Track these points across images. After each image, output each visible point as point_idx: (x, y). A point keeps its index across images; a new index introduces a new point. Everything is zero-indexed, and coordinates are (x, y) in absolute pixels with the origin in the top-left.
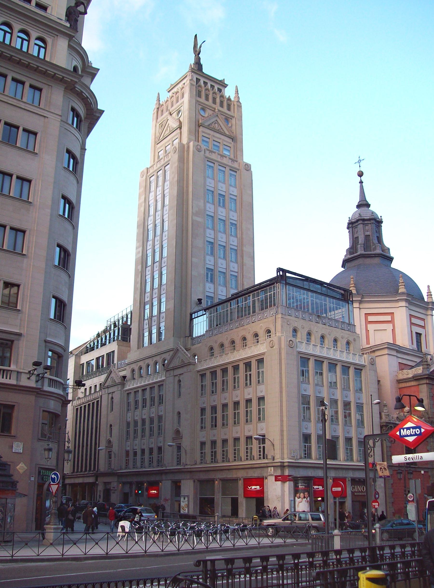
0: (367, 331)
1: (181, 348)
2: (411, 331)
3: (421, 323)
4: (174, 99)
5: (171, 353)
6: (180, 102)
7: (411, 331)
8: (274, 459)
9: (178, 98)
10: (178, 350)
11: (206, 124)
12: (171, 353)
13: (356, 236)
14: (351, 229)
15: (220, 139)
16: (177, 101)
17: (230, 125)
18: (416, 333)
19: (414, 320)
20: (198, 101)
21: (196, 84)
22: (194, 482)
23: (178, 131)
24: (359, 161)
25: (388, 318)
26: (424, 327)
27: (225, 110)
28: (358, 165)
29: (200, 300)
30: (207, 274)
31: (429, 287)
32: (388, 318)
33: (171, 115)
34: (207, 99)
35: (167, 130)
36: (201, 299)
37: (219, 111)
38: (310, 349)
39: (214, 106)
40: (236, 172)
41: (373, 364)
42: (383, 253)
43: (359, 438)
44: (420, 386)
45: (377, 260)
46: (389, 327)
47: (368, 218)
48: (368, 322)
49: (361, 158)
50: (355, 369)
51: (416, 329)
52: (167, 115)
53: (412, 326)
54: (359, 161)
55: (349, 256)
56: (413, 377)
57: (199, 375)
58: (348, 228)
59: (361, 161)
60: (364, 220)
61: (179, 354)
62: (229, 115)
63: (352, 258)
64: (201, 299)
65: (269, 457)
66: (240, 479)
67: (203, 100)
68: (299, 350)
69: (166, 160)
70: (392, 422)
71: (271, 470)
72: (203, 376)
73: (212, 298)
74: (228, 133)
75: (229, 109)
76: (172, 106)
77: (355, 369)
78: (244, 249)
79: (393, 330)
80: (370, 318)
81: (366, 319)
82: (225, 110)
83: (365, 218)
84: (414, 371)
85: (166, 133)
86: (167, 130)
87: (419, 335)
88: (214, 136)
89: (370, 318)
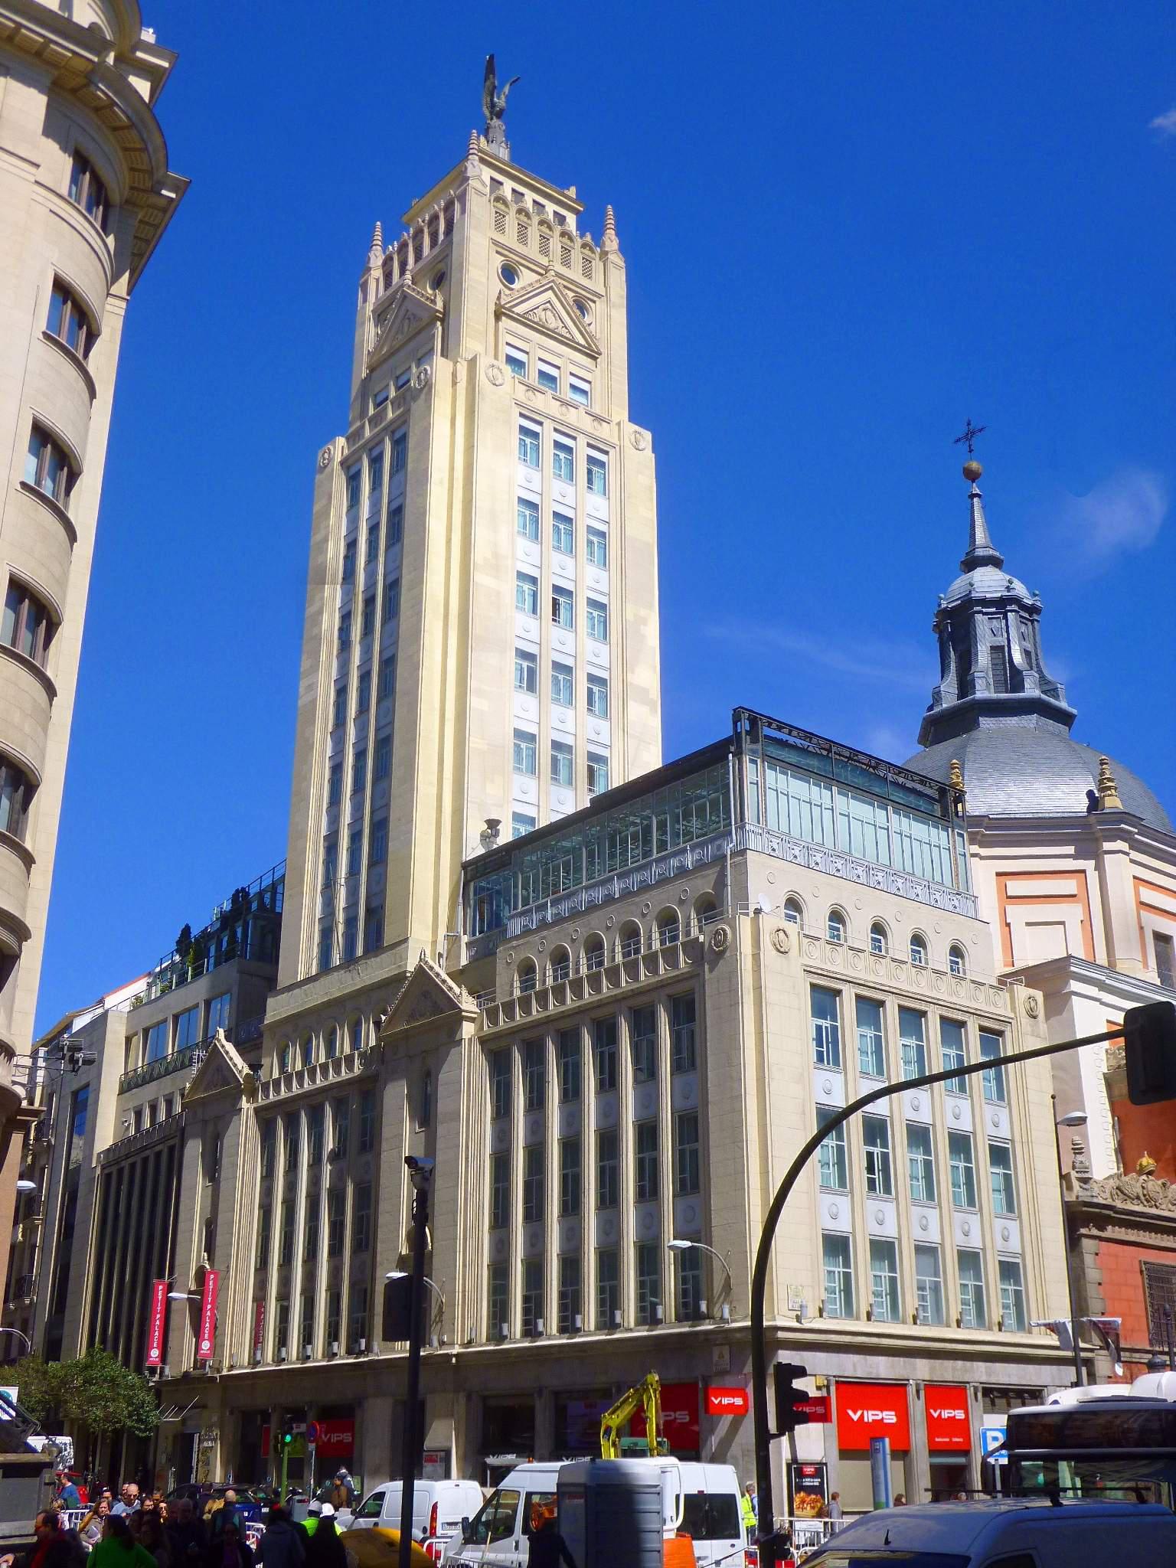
2: (1142, 928)
11: (519, 310)
15: (560, 356)
17: (587, 319)
20: (496, 243)
21: (491, 192)
22: (469, 1398)
24: (969, 435)
25: (1069, 886)
29: (493, 824)
30: (517, 746)
32: (1069, 886)
34: (523, 237)
36: (498, 822)
37: (558, 275)
38: (838, 963)
39: (544, 261)
41: (1035, 1017)
42: (1043, 696)
45: (1032, 720)
46: (1072, 913)
50: (982, 1029)
54: (969, 435)
59: (973, 433)
60: (985, 602)
62: (584, 288)
64: (498, 822)
67: (510, 238)
70: (1101, 1201)
71: (721, 1356)
73: (532, 821)
74: (583, 342)
75: (587, 273)
77: (982, 1029)
79: (1087, 923)
80: (1016, 887)
82: (575, 273)
83: (988, 596)
87: (1161, 939)
89: (1016, 887)
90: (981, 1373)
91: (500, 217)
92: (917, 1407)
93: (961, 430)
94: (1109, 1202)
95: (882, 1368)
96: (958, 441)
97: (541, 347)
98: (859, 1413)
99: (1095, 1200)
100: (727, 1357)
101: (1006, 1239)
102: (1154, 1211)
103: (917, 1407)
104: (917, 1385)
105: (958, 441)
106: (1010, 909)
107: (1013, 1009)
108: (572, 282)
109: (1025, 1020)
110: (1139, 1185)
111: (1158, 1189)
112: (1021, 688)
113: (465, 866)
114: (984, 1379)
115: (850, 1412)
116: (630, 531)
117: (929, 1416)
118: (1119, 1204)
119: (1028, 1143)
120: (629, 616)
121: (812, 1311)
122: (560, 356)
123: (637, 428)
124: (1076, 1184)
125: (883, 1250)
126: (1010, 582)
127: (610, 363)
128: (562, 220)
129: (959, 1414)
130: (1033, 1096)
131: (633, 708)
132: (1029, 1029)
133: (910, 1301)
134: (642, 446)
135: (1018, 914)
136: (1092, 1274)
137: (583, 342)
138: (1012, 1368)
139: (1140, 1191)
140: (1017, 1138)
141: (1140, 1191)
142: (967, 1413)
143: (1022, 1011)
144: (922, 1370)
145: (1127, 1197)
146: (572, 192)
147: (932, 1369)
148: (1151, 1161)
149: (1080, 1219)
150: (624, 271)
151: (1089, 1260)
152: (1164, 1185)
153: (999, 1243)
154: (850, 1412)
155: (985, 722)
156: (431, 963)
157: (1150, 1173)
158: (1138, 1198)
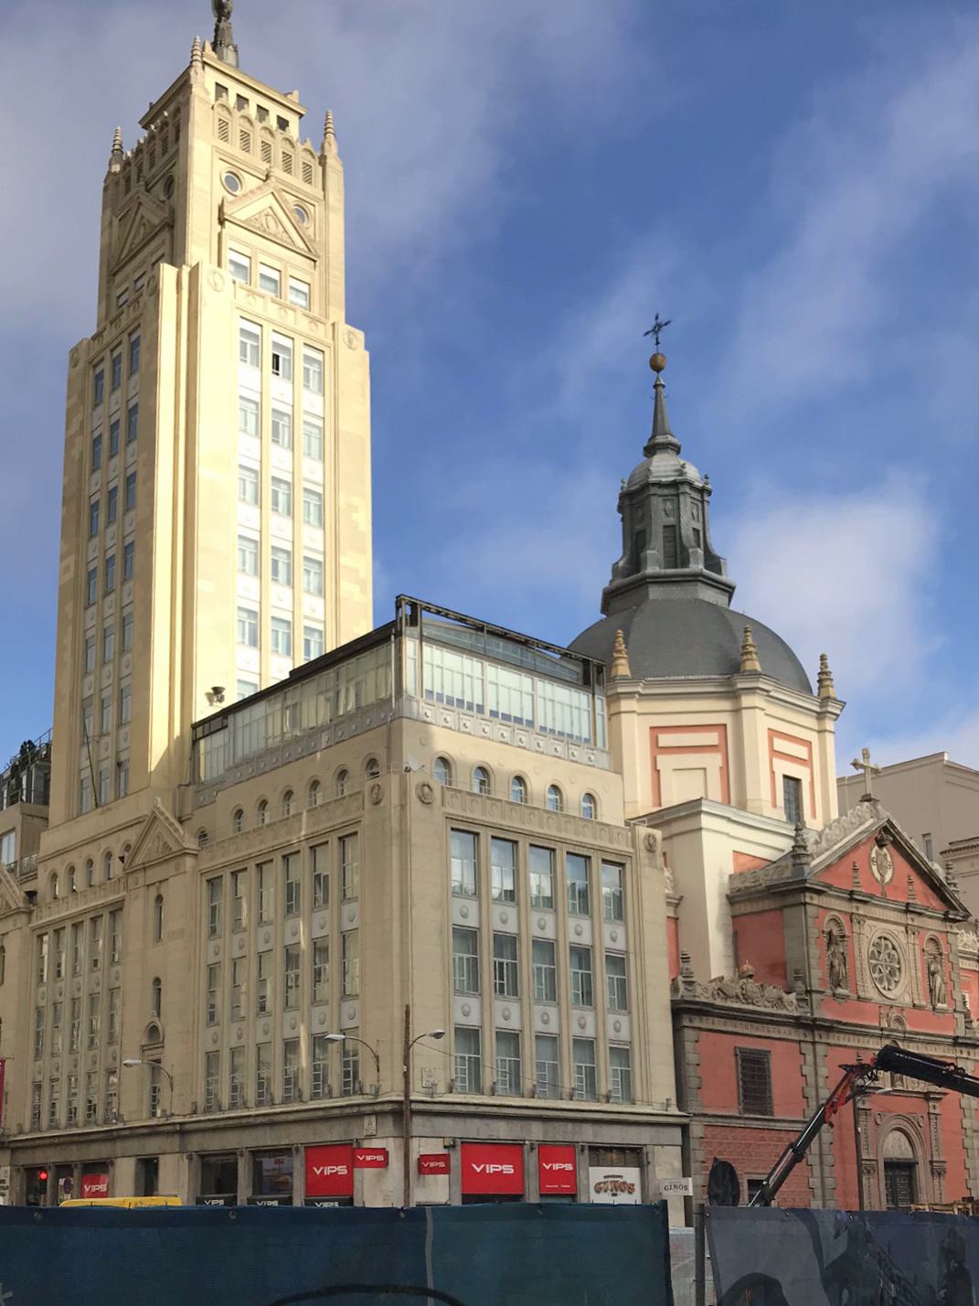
0: (657, 772)
1: (162, 813)
2: (773, 772)
3: (801, 752)
4: (158, 143)
5: (138, 829)
6: (171, 151)
7: (773, 772)
8: (377, 1094)
9: (165, 141)
10: (155, 817)
12: (138, 829)
13: (638, 527)
14: (627, 511)
16: (165, 151)
18: (786, 777)
19: (780, 745)
23: (165, 235)
24: (657, 328)
25: (712, 738)
26: (806, 762)
27: (296, 180)
28: (651, 339)
31: (823, 658)
32: (712, 738)
33: (148, 191)
34: (246, 147)
35: (138, 232)
40: (323, 352)
43: (612, 1041)
44: (786, 911)
46: (714, 761)
47: (672, 479)
48: (657, 749)
49: (662, 319)
51: (784, 768)
52: (137, 192)
53: (776, 761)
55: (620, 581)
56: (769, 888)
57: (204, 882)
58: (620, 509)
60: (660, 485)
61: (157, 829)
62: (305, 193)
63: (632, 583)
65: (367, 1090)
66: (297, 1149)
68: (448, 810)
69: (132, 316)
70: (703, 999)
71: (370, 1124)
72: (213, 883)
76: (152, 164)
78: (343, 560)
79: (725, 770)
80: (665, 740)
81: (655, 741)
83: (664, 480)
84: (771, 872)
85: (137, 241)
86: (138, 232)
88: (264, 252)
89: (665, 740)
90: (588, 1134)
91: (223, 127)
92: (532, 1160)
93: (650, 325)
94: (710, 1001)
95: (502, 1131)
96: (648, 333)
97: (264, 252)
98: (482, 1166)
99: (697, 999)
100: (374, 1123)
101: (618, 1030)
102: (751, 1007)
103: (532, 1160)
104: (532, 1144)
105: (648, 333)
106: (660, 758)
107: (634, 846)
108: (291, 187)
109: (643, 854)
110: (738, 986)
111: (755, 989)
112: (685, 563)
113: (195, 726)
114: (590, 1140)
115: (474, 1166)
116: (342, 426)
117: (541, 1169)
118: (719, 1002)
119: (641, 953)
120: (342, 504)
121: (441, 1088)
122: (280, 259)
123: (349, 327)
124: (682, 987)
125: (510, 1039)
126: (683, 466)
127: (327, 266)
128: (283, 124)
129: (569, 1167)
130: (647, 916)
131: (345, 586)
132: (647, 861)
133: (529, 1079)
134: (355, 343)
135: (665, 762)
136: (691, 1057)
137: (301, 244)
138: (616, 1130)
139: (739, 991)
140: (631, 950)
141: (739, 991)
142: (575, 1167)
143: (642, 846)
144: (536, 1132)
145: (727, 997)
146: (295, 96)
147: (545, 1133)
148: (750, 968)
149: (681, 1011)
150: (341, 175)
151: (689, 1046)
152: (762, 986)
153: (611, 1033)
154: (474, 1166)
155: (655, 592)
156: (163, 809)
157: (751, 976)
158: (737, 997)
